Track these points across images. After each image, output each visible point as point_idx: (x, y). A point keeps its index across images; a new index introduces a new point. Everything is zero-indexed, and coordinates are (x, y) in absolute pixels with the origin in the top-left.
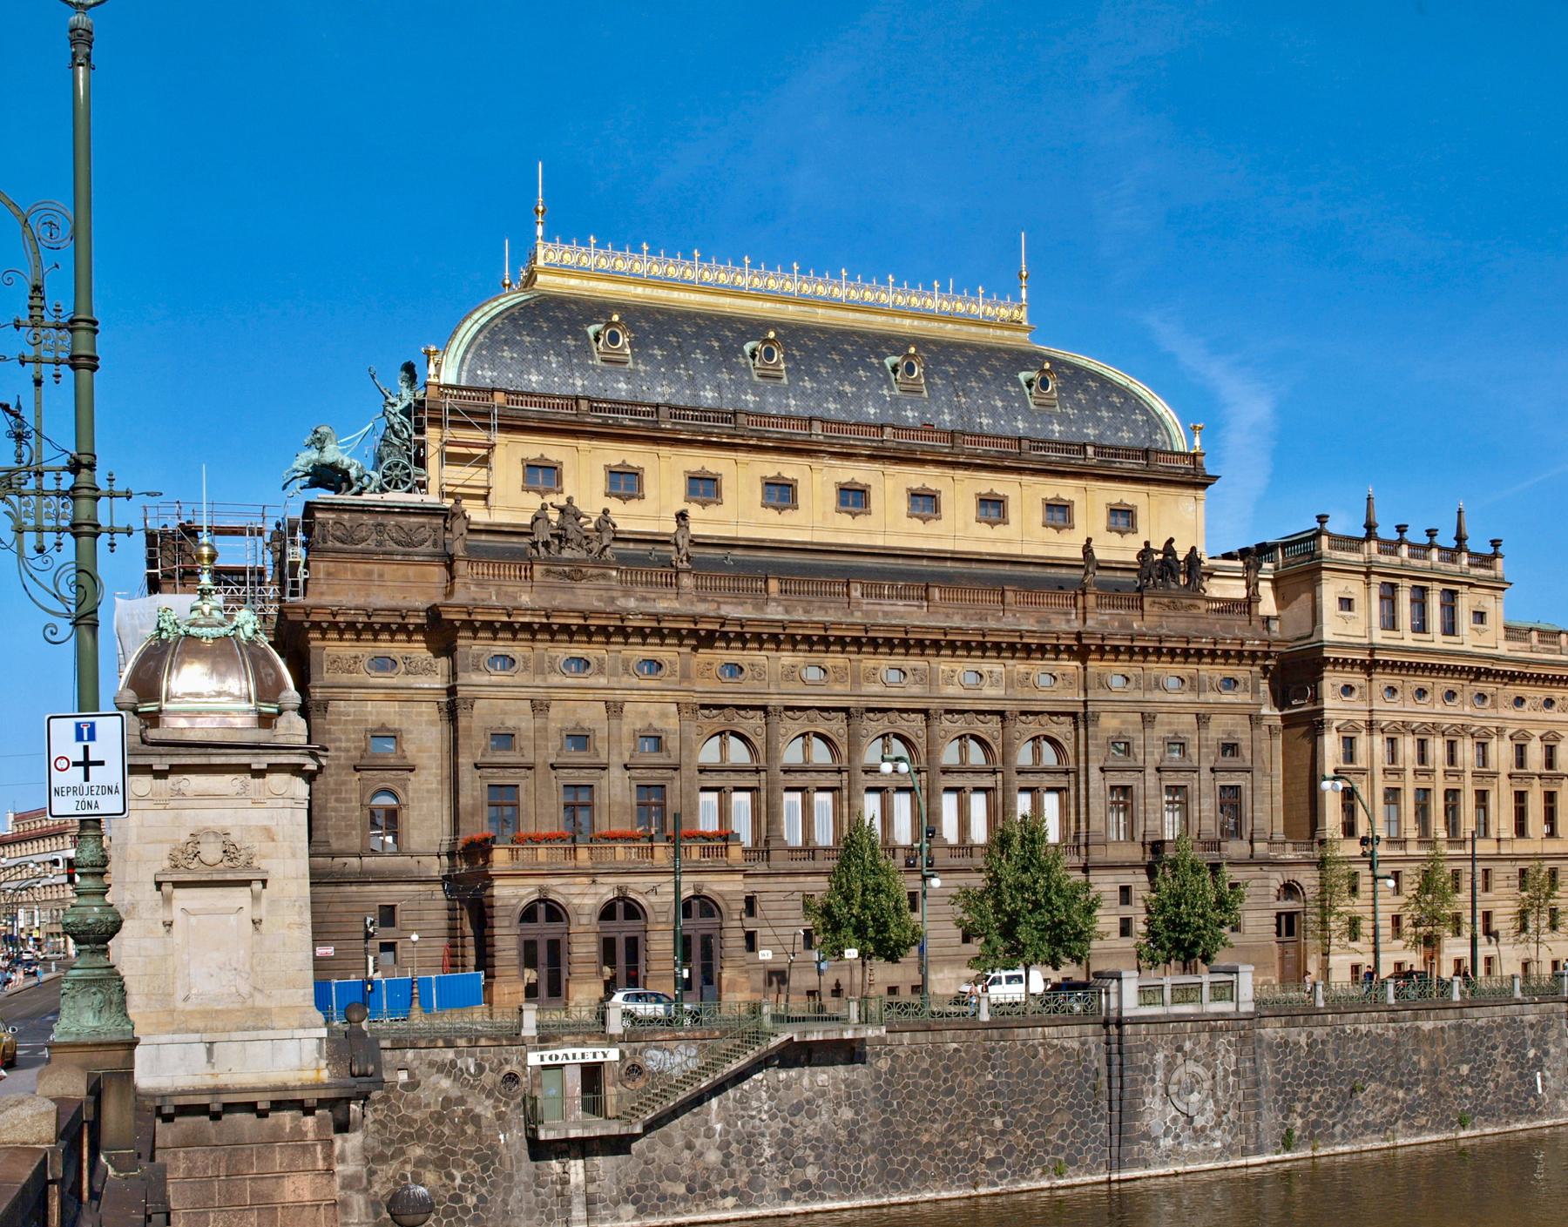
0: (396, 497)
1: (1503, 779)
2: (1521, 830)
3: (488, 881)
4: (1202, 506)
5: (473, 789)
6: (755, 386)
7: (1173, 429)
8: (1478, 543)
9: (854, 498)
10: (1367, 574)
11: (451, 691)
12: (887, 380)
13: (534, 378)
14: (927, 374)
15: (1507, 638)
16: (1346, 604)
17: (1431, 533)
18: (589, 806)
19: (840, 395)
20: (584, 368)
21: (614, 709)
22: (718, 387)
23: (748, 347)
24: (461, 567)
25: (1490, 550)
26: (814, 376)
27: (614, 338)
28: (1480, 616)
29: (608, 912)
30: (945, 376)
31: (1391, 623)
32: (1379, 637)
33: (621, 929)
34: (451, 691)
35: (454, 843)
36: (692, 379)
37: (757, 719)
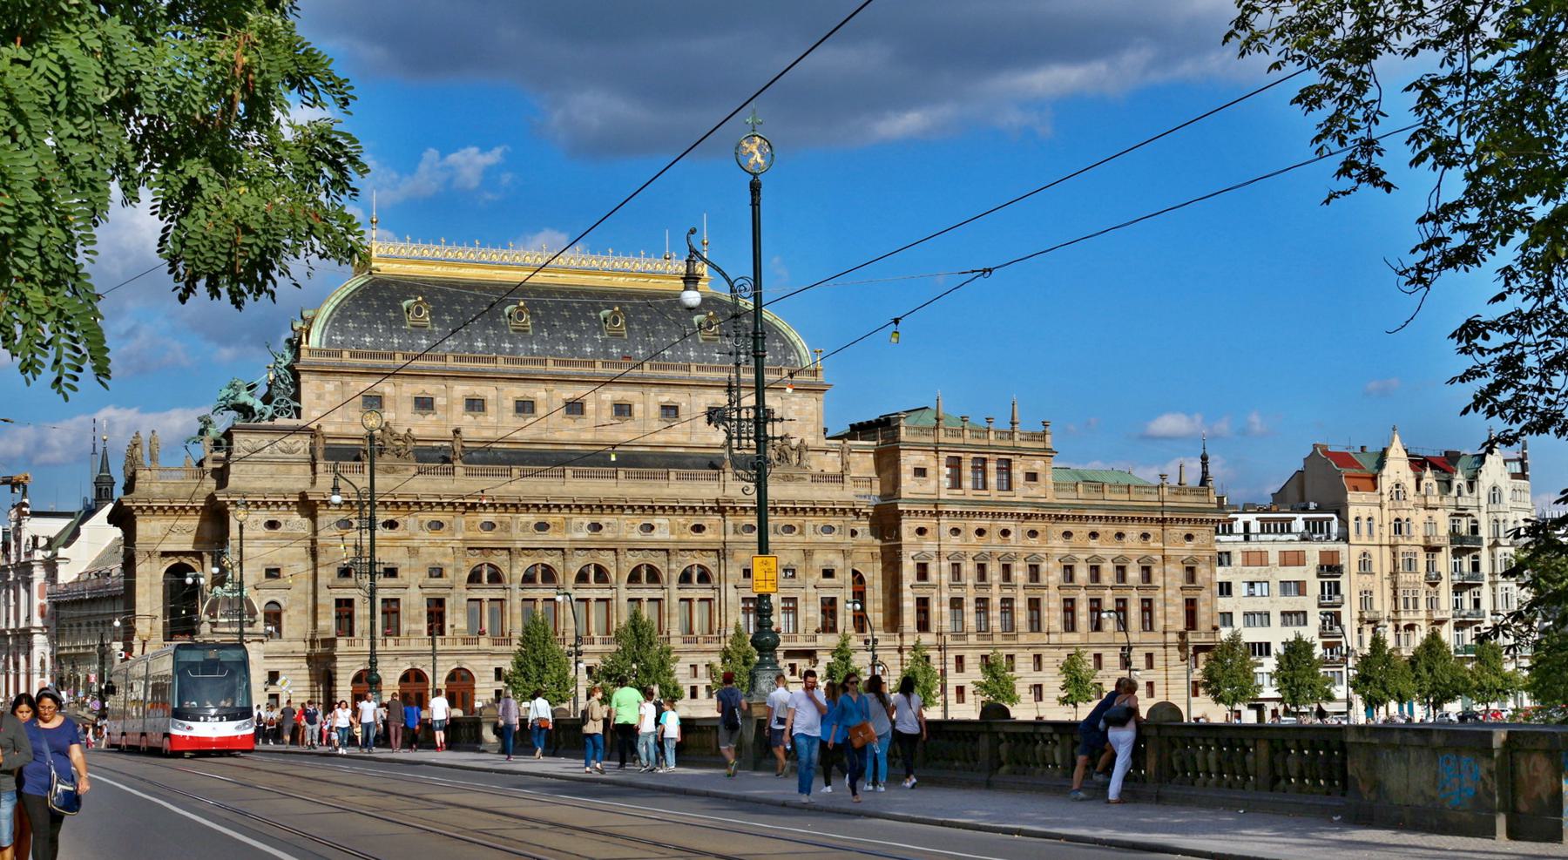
0: (281, 421)
1: (1052, 590)
2: (1070, 626)
3: (334, 658)
4: (821, 404)
5: (327, 600)
6: (511, 337)
7: (802, 352)
8: (1028, 424)
9: (575, 408)
10: (937, 451)
11: (314, 542)
12: (600, 328)
14: (627, 323)
15: (1056, 490)
16: (920, 472)
17: (989, 420)
18: (397, 612)
19: (567, 340)
20: (399, 330)
21: (413, 552)
22: (486, 339)
23: (507, 311)
24: (320, 467)
25: (1040, 429)
26: (551, 328)
27: (419, 311)
28: (1032, 477)
29: (405, 678)
30: (641, 322)
31: (956, 482)
32: (944, 495)
33: (413, 687)
34: (314, 542)
35: (313, 635)
36: (469, 334)
37: (504, 555)
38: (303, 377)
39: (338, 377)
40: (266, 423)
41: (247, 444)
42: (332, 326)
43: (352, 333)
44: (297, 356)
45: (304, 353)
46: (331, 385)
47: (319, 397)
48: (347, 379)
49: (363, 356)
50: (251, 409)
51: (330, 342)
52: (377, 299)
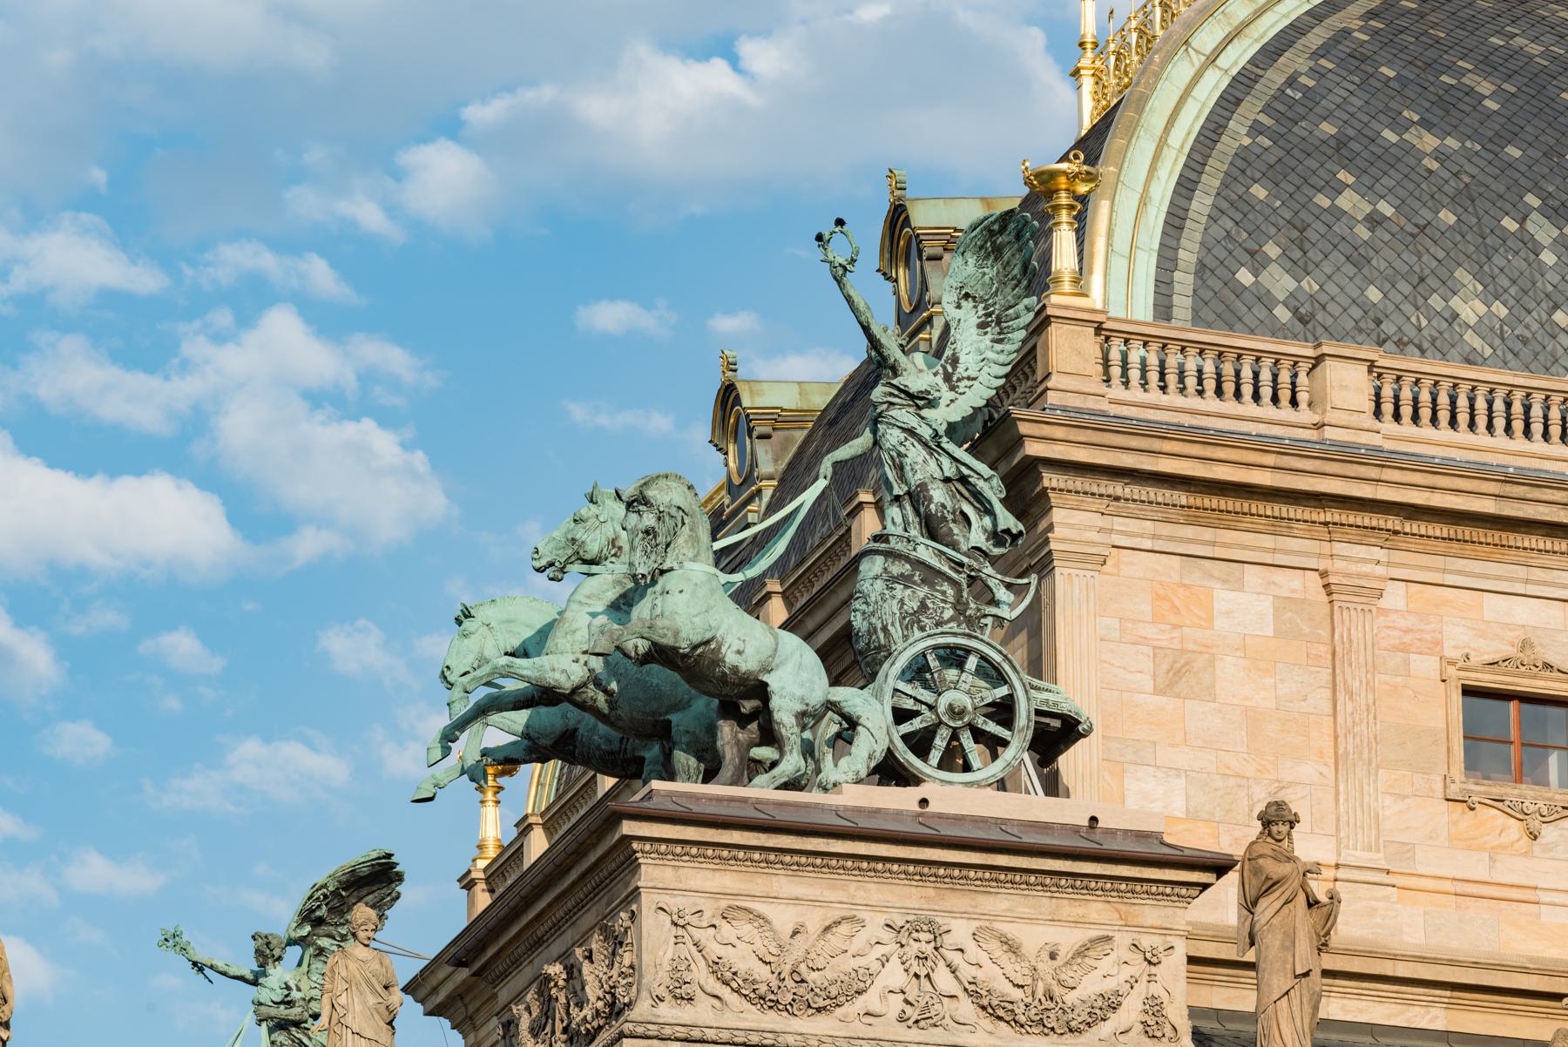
0: (950, 796)
13: (1470, 309)
38: (1072, 522)
39: (1299, 547)
40: (847, 788)
41: (742, 950)
42: (1232, 203)
43: (1358, 259)
44: (1025, 373)
45: (1070, 353)
46: (1251, 595)
47: (1179, 673)
48: (1358, 559)
49: (1449, 411)
50: (745, 698)
51: (1221, 301)
52: (1488, 64)
